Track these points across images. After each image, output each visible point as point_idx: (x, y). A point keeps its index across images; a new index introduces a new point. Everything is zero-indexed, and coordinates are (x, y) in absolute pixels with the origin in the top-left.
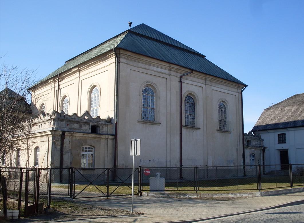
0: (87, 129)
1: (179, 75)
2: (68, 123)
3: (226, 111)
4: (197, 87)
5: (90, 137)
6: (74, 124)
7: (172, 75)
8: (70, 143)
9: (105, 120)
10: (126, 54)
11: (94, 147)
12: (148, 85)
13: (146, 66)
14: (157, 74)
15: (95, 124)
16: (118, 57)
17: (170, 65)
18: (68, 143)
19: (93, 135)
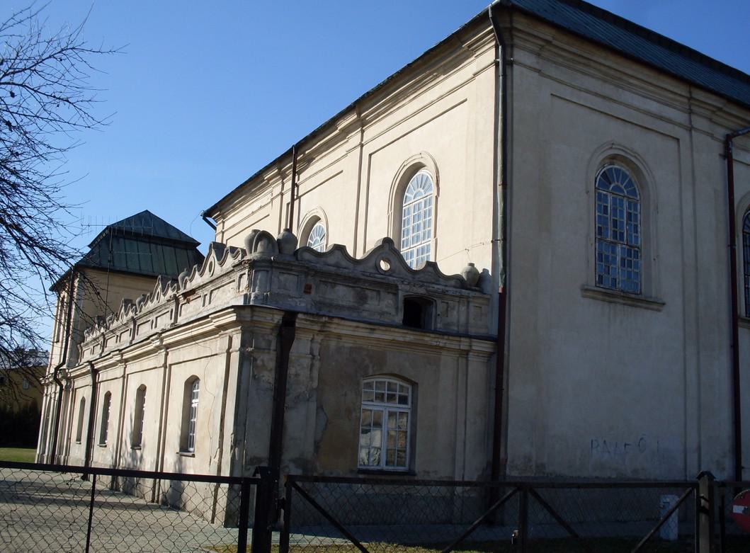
0: (386, 310)
1: (721, 132)
2: (310, 280)
5: (398, 342)
6: (334, 285)
7: (697, 130)
8: (317, 364)
9: (457, 278)
10: (536, 33)
11: (414, 384)
12: (613, 158)
13: (608, 90)
14: (649, 122)
15: (422, 291)
16: (505, 43)
17: (690, 93)
18: (306, 362)
19: (410, 336)
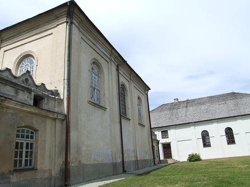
0: (27, 99)
1: (117, 64)
5: (32, 112)
11: (36, 131)
19: (36, 111)
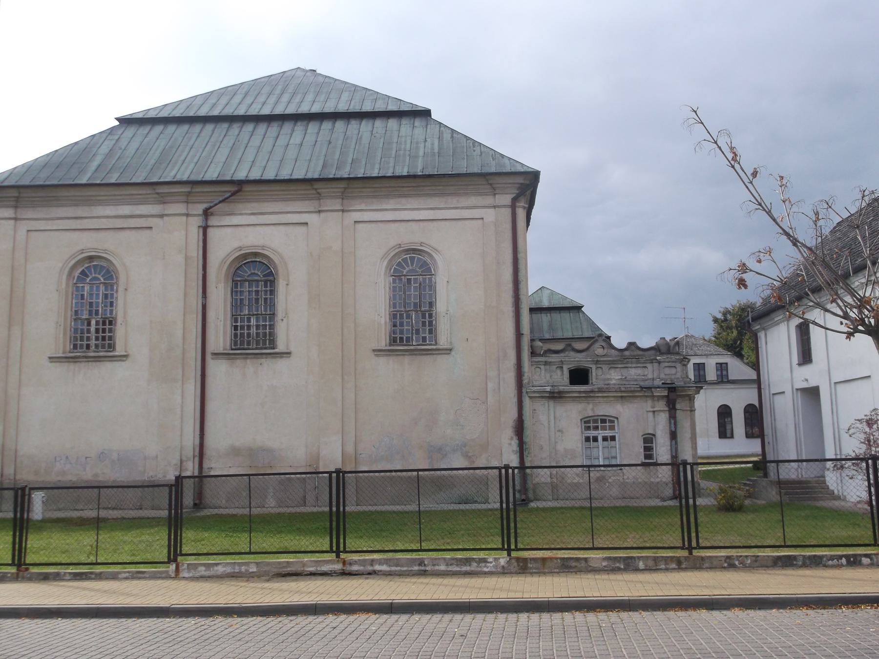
1: (199, 208)
3: (430, 279)
4: (282, 228)
13: (81, 211)
14: (119, 223)
